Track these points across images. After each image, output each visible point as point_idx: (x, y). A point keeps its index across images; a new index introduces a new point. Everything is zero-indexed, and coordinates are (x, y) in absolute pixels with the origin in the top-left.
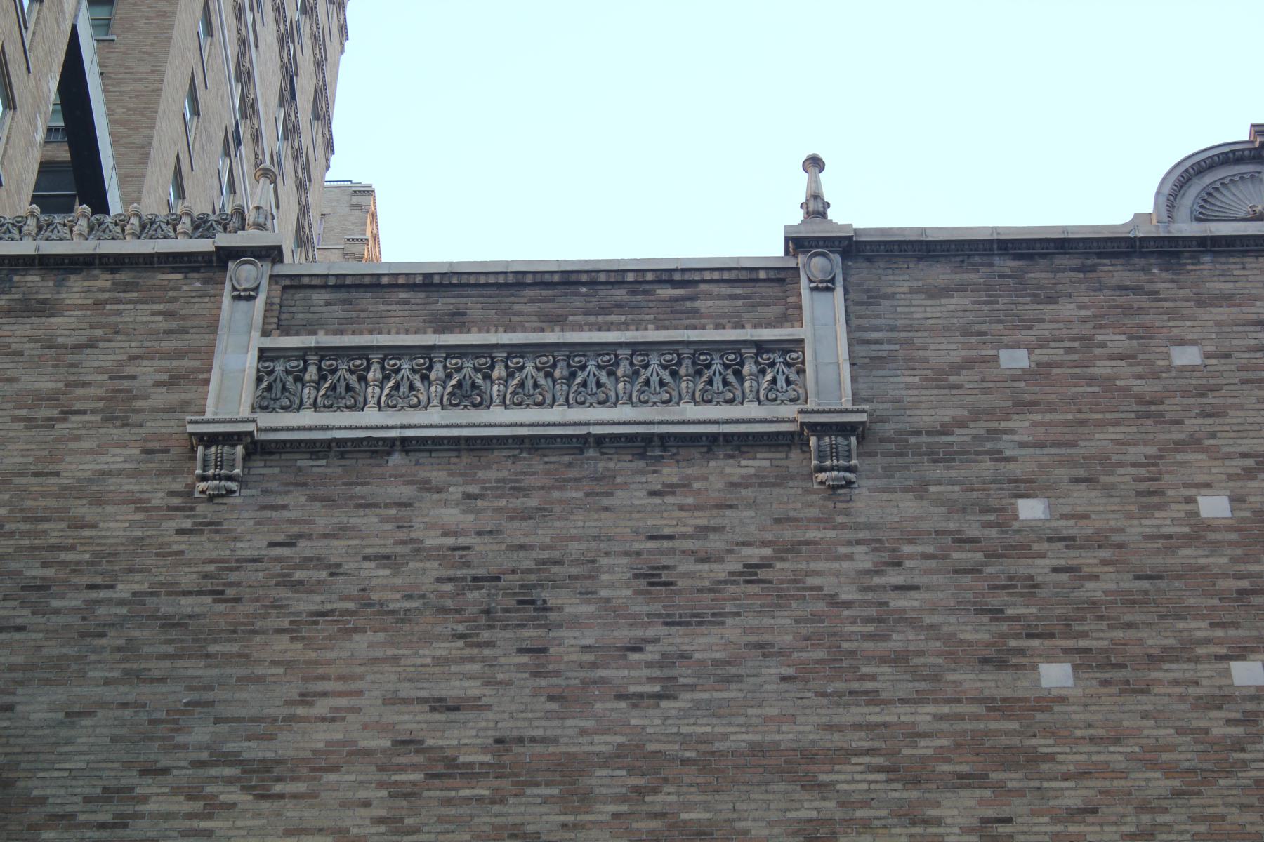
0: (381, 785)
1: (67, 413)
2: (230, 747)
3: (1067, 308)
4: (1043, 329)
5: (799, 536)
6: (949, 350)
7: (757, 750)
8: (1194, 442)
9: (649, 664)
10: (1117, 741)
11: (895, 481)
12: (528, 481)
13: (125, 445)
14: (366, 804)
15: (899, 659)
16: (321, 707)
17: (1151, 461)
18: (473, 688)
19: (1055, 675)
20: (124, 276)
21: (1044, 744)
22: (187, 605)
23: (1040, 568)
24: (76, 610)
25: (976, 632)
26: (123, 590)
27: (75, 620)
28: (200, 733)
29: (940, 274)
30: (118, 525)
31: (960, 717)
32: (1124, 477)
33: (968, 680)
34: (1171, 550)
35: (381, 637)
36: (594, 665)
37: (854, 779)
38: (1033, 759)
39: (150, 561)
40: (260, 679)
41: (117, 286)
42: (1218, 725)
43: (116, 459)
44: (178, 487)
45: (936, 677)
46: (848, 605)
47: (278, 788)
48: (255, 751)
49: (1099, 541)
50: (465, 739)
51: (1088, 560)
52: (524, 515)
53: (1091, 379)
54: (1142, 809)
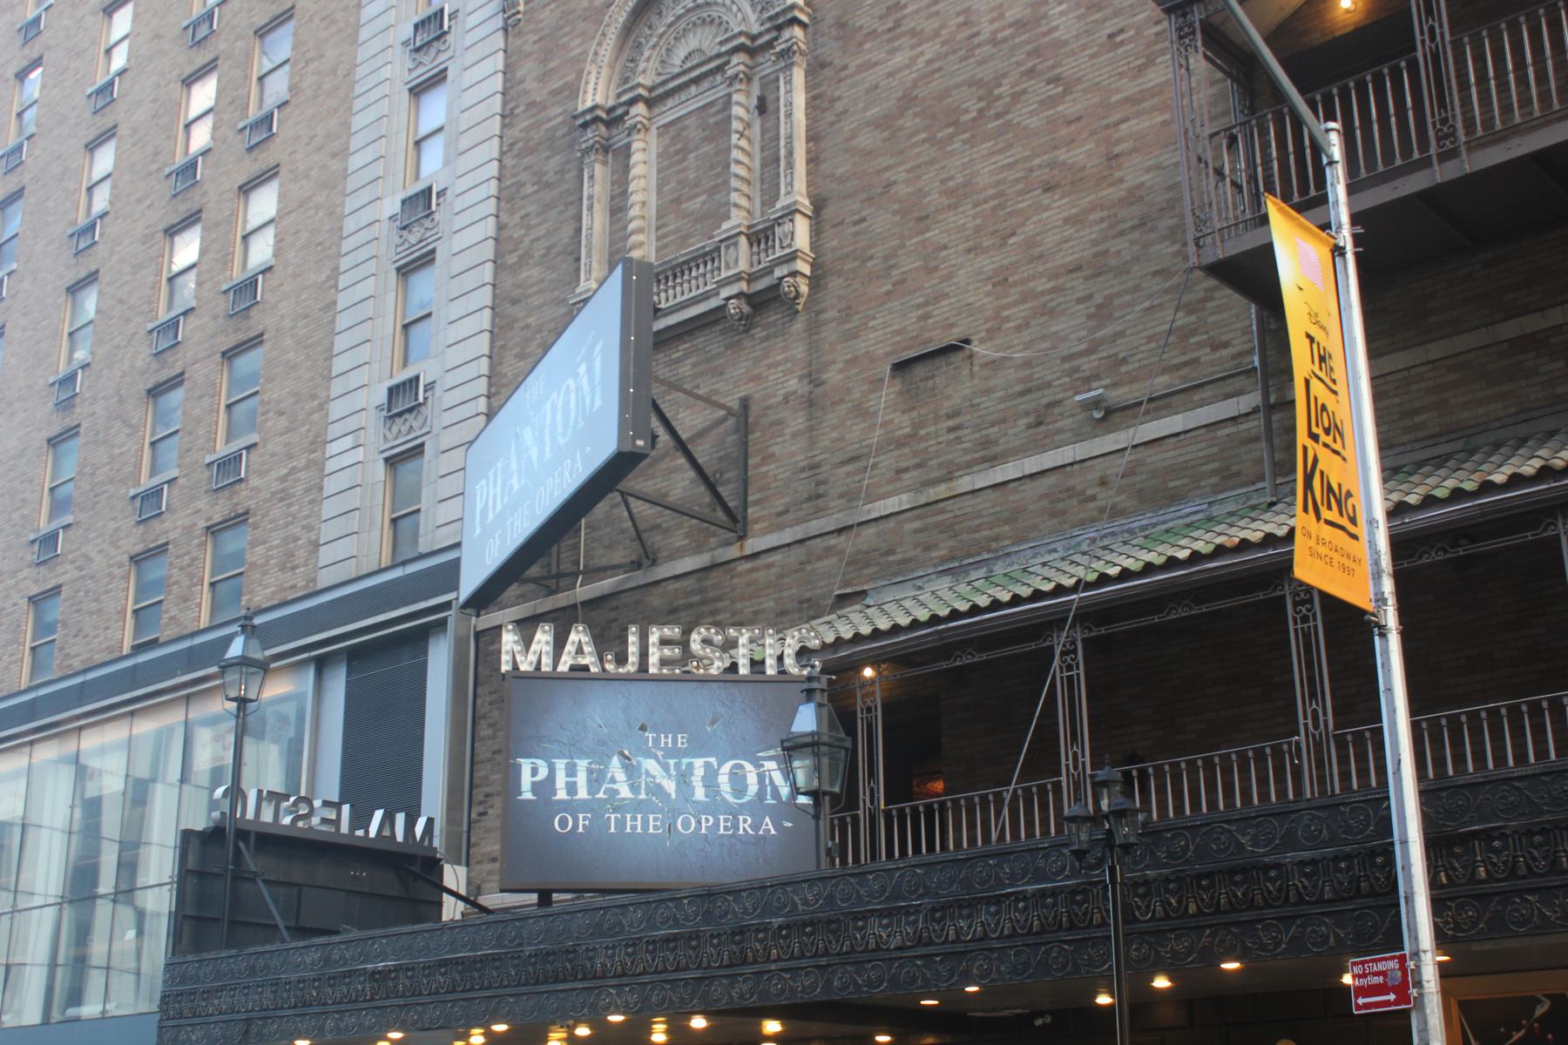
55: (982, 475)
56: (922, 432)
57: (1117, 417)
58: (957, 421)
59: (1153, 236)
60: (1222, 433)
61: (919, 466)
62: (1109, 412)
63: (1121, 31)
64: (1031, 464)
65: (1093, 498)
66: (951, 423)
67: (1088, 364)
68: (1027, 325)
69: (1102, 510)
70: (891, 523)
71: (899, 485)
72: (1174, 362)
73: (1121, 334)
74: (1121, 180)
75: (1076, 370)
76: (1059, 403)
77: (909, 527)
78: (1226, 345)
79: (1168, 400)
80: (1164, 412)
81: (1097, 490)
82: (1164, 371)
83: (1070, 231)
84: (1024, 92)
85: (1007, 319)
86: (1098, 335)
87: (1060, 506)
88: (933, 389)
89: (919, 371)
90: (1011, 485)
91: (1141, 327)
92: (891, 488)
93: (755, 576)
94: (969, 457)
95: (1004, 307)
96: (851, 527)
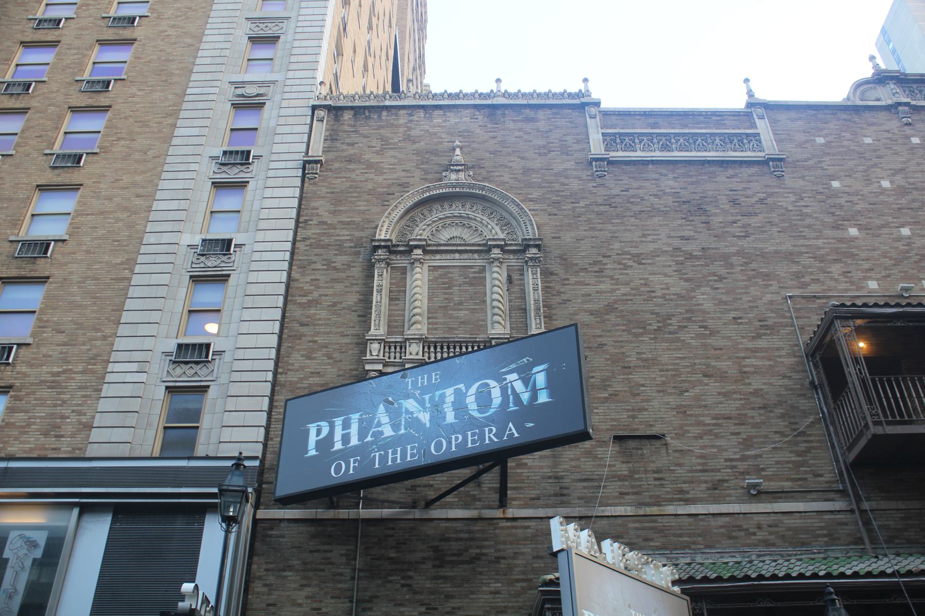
0: (673, 261)
1: (550, 151)
2: (626, 249)
3: (831, 126)
4: (825, 132)
5: (772, 191)
6: (801, 137)
7: (776, 252)
8: (875, 166)
9: (739, 227)
10: (874, 250)
11: (795, 175)
12: (691, 173)
13: (569, 161)
14: (670, 266)
15: (809, 226)
16: (650, 238)
17: (865, 171)
18: (692, 233)
19: (853, 232)
20: (554, 111)
21: (854, 251)
22: (602, 208)
23: (842, 201)
24: (569, 210)
25: (829, 219)
26: (582, 204)
27: (571, 212)
28: (617, 245)
29: (793, 114)
30: (575, 185)
31: (830, 243)
32: (858, 175)
33: (829, 232)
34: (877, 197)
35: (661, 218)
36: (724, 227)
37: (806, 260)
38: (853, 256)
39: (588, 195)
40: (629, 230)
41: (553, 114)
42: (901, 246)
43: (570, 165)
44: (589, 173)
45: (820, 232)
46: (791, 211)
47: (644, 261)
48: (634, 251)
49: (856, 193)
50: (691, 247)
51: (855, 199)
52: (692, 183)
53: (843, 146)
54: (886, 269)
56: (637, 476)
57: (763, 496)
58: (659, 475)
59: (772, 414)
60: (825, 517)
61: (636, 493)
62: (760, 492)
63: (740, 318)
65: (754, 534)
66: (656, 475)
68: (701, 438)
69: (759, 540)
70: (619, 521)
71: (622, 501)
73: (760, 456)
74: (750, 384)
75: (735, 467)
76: (727, 481)
77: (631, 525)
78: (821, 476)
81: (756, 530)
82: (788, 480)
83: (721, 399)
84: (686, 327)
85: (688, 431)
87: (734, 534)
88: (642, 455)
89: (632, 444)
92: (616, 501)
93: (514, 531)
94: (670, 496)
95: (686, 425)
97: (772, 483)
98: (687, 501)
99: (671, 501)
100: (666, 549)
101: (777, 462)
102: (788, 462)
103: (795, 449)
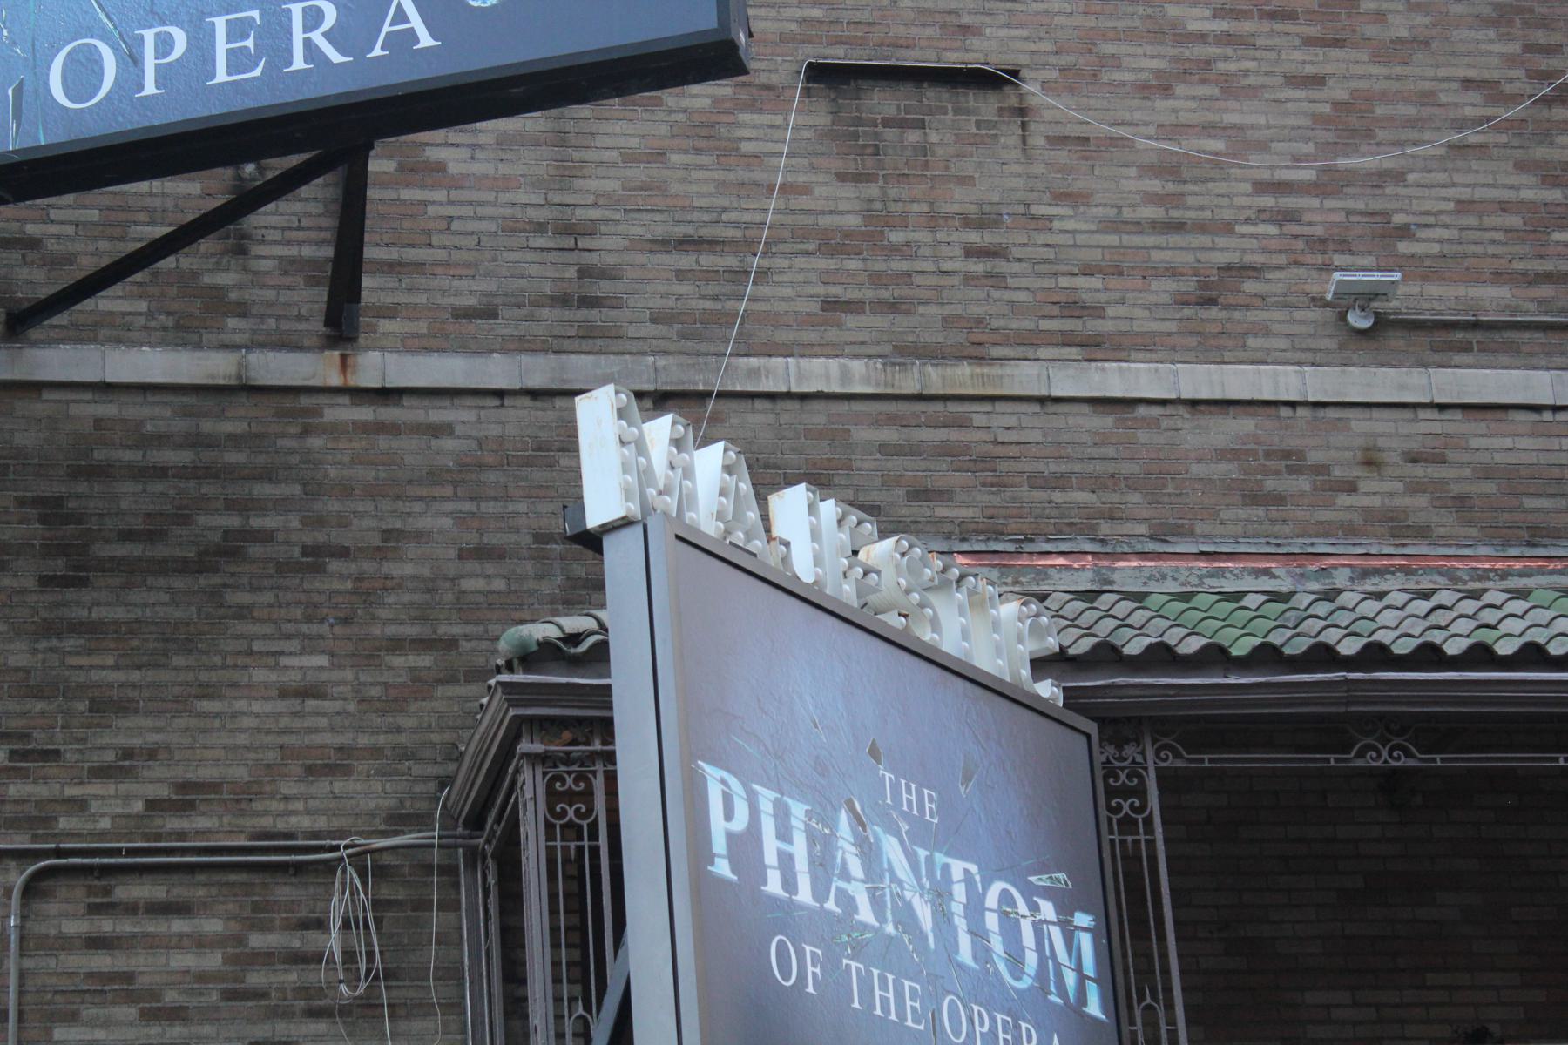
55: (1072, 369)
56: (896, 237)
57: (1396, 340)
58: (989, 238)
61: (893, 307)
62: (1382, 322)
64: (1198, 380)
65: (1351, 488)
66: (973, 237)
67: (1321, 214)
68: (1166, 90)
69: (1367, 512)
70: (817, 415)
71: (832, 334)
72: (1518, 266)
73: (1398, 176)
75: (1290, 216)
76: (1256, 271)
77: (864, 435)
79: (1510, 335)
80: (1504, 359)
81: (1357, 472)
82: (1498, 277)
85: (1115, 61)
86: (1342, 162)
87: (1270, 484)
89: (882, 102)
90: (1142, 410)
91: (1441, 177)
92: (809, 336)
93: (383, 442)
94: (1027, 324)
96: (704, 396)
97: (1433, 290)
98: (1094, 348)
99: (1029, 342)
100: (998, 534)
101: (1463, 206)
102: (1504, 207)
103: (1540, 152)
